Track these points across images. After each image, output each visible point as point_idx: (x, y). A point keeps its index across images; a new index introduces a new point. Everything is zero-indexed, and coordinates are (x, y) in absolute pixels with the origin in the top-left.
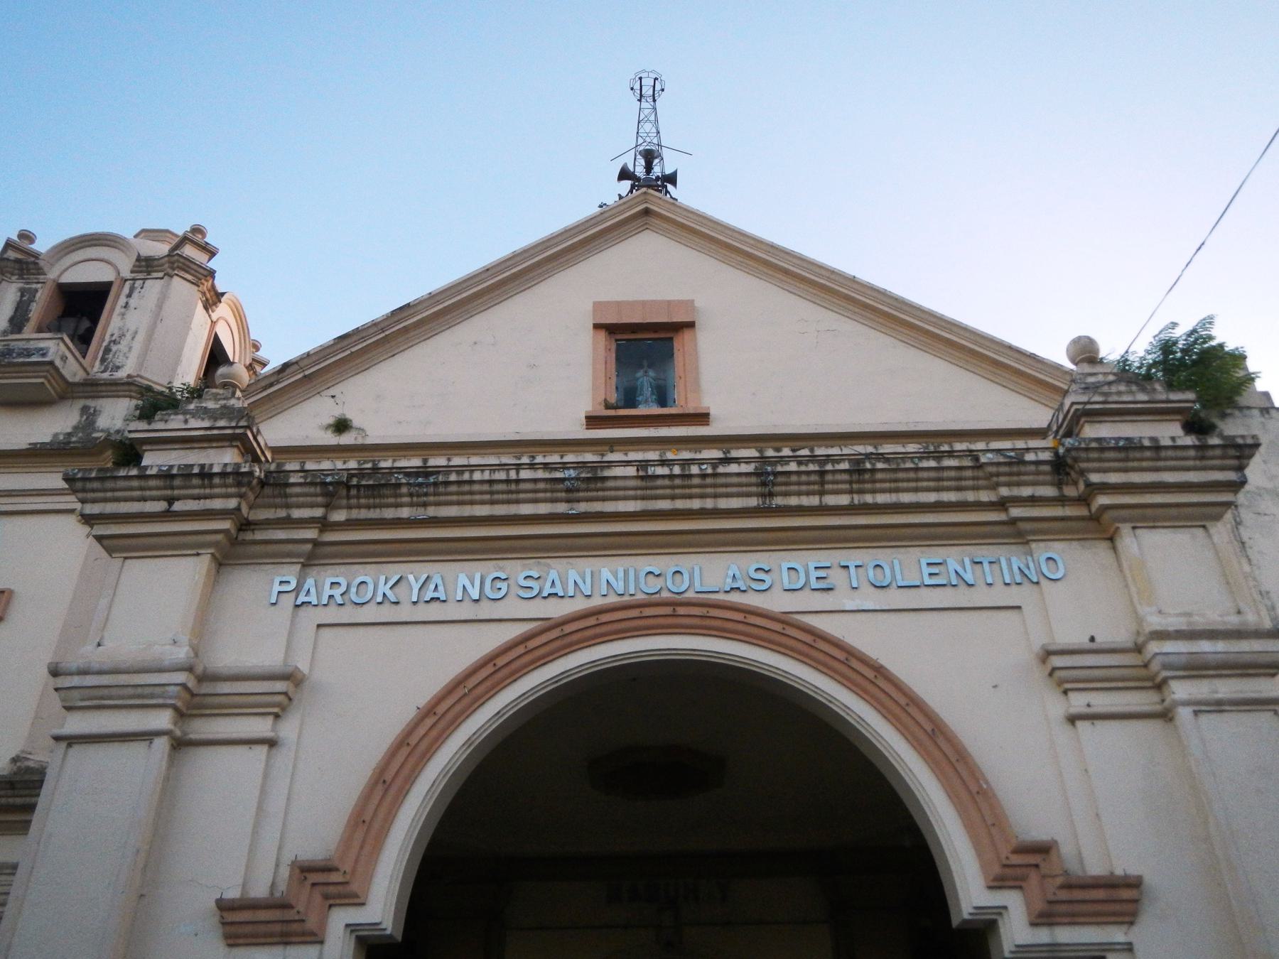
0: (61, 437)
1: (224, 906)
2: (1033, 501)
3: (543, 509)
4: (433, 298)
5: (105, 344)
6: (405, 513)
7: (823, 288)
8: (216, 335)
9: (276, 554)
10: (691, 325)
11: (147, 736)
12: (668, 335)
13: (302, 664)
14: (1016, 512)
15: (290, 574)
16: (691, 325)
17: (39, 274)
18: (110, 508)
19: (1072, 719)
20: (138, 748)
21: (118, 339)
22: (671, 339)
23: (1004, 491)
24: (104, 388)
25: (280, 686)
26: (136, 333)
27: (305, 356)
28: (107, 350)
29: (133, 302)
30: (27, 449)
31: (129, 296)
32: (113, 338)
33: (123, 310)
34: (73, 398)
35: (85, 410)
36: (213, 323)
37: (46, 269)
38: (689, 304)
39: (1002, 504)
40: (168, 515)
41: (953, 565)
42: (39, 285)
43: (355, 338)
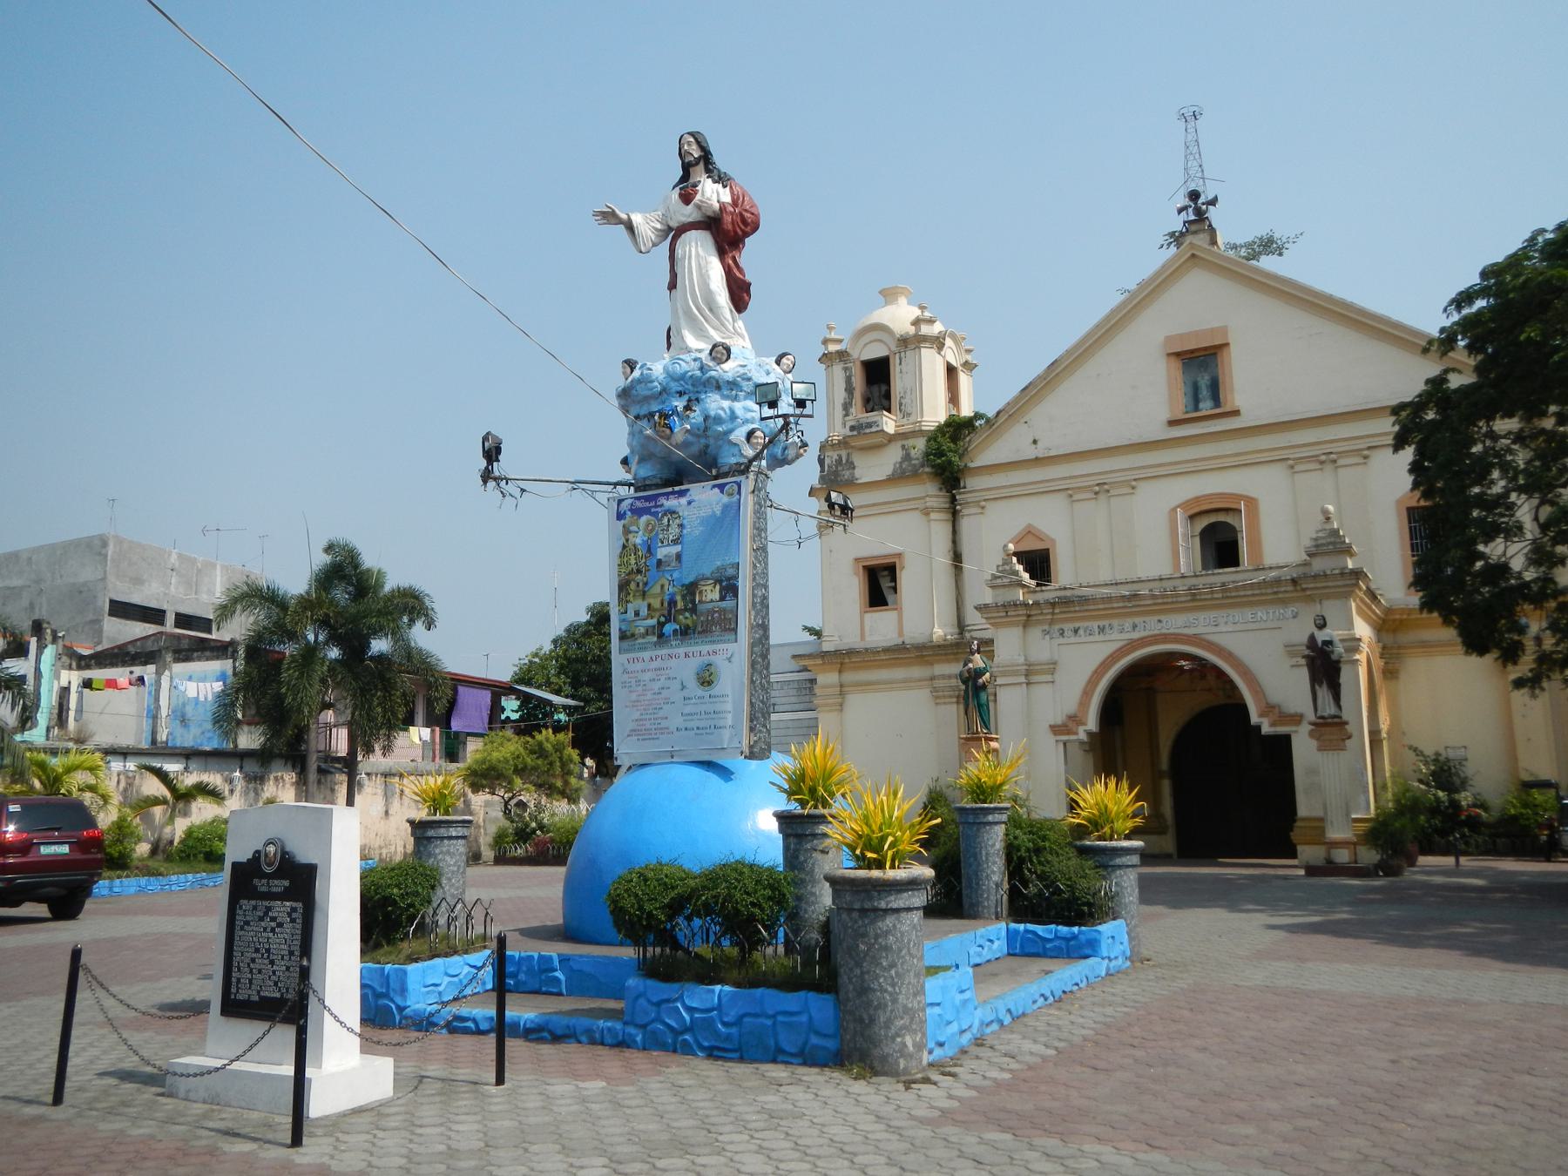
1: (1050, 726)
2: (1286, 592)
3: (1121, 604)
4: (1069, 352)
6: (1077, 609)
7: (1313, 304)
8: (948, 363)
9: (1039, 622)
10: (1227, 345)
11: (1020, 684)
12: (1212, 352)
13: (1056, 658)
14: (1280, 596)
15: (1046, 627)
16: (1227, 345)
18: (990, 615)
19: (1293, 666)
20: (1018, 688)
22: (1215, 354)
23: (1275, 590)
25: (1052, 666)
28: (901, 404)
31: (900, 364)
35: (903, 447)
36: (944, 357)
38: (1224, 330)
39: (1276, 593)
40: (1007, 616)
41: (1259, 614)
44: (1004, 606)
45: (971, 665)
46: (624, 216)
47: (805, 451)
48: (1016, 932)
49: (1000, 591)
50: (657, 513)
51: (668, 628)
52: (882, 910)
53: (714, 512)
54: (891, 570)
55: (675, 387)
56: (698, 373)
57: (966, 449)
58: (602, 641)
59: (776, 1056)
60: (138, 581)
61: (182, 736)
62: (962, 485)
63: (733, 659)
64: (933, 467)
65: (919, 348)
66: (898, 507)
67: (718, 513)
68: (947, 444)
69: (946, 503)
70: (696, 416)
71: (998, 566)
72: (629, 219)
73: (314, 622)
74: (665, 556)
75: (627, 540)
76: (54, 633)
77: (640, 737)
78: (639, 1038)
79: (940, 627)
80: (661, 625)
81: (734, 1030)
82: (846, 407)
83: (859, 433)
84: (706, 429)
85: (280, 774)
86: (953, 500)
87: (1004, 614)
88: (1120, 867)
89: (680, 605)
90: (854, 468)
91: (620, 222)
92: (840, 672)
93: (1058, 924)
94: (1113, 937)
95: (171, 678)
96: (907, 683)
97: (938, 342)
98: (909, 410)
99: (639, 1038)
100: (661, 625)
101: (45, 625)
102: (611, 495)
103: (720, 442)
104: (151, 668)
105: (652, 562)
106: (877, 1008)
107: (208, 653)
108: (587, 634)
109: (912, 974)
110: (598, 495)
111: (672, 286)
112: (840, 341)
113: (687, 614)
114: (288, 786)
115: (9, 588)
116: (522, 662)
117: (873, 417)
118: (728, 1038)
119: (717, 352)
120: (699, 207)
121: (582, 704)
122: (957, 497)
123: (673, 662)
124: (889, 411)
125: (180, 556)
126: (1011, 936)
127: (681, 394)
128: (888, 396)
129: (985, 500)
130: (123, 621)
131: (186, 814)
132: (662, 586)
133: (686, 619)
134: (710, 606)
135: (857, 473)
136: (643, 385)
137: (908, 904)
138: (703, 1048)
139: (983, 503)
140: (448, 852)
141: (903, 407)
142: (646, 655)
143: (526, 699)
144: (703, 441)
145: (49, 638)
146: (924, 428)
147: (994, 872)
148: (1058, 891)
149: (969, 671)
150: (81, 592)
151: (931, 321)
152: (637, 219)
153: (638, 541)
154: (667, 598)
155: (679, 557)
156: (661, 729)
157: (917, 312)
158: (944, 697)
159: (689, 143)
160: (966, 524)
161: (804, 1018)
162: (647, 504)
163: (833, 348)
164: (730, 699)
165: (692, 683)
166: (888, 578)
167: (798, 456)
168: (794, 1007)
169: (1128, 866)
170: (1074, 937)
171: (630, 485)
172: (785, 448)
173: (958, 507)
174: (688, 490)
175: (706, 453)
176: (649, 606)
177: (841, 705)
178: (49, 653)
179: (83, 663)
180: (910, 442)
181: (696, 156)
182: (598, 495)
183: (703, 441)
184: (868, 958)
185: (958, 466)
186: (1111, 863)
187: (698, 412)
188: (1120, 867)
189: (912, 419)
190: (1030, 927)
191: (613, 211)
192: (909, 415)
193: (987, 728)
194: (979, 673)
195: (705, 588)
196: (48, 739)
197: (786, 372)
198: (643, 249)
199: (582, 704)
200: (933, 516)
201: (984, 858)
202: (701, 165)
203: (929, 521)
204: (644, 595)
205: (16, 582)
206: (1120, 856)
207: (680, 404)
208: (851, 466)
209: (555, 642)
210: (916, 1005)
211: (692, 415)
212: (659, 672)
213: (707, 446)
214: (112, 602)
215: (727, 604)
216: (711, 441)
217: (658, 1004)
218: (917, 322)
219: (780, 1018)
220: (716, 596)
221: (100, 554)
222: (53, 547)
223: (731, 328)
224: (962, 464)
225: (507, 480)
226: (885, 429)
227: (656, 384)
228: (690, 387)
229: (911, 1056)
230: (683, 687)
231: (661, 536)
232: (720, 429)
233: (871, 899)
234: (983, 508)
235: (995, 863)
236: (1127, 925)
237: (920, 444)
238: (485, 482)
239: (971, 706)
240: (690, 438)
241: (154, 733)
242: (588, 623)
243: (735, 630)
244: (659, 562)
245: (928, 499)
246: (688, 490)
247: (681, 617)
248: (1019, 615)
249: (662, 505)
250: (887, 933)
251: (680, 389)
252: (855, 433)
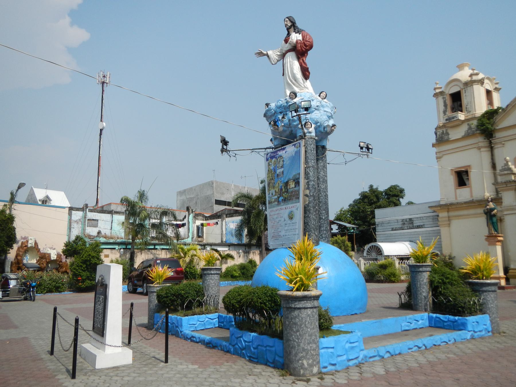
0: (466, 132)
5: (465, 106)
26: (470, 102)
28: (466, 108)
29: (467, 94)
31: (465, 93)
33: (465, 97)
35: (468, 124)
40: (507, 186)
44: (505, 182)
45: (488, 207)
46: (265, 53)
47: (335, 128)
48: (432, 317)
49: (504, 177)
50: (277, 157)
51: (281, 199)
52: (293, 308)
53: (292, 155)
54: (467, 172)
55: (278, 110)
56: (286, 104)
57: (494, 122)
58: (364, 205)
59: (266, 363)
60: (223, 194)
61: (232, 240)
62: (494, 136)
63: (298, 209)
64: (481, 130)
65: (472, 85)
66: (468, 147)
67: (294, 155)
68: (485, 121)
69: (487, 144)
70: (286, 120)
71: (502, 167)
72: (267, 53)
73: (261, 203)
74: (279, 173)
75: (269, 168)
76: (192, 210)
77: (274, 239)
78: (232, 350)
79: (488, 193)
80: (279, 198)
81: (256, 351)
82: (445, 112)
83: (449, 121)
84: (290, 124)
85: (254, 251)
86: (490, 143)
87: (505, 186)
88: (486, 291)
89: (284, 190)
90: (449, 135)
91: (264, 55)
92: (448, 212)
93: (450, 315)
94: (477, 322)
95: (226, 222)
96: (475, 215)
97: (481, 82)
98: (470, 110)
99: (232, 350)
100: (279, 198)
101: (190, 208)
102: (264, 153)
103: (296, 129)
104: (220, 220)
105: (276, 175)
106: (292, 348)
107: (237, 214)
108: (359, 203)
109: (307, 335)
110: (260, 153)
111: (283, 75)
112: (441, 88)
113: (286, 193)
114: (257, 255)
115: (191, 198)
116: (338, 213)
117: (454, 114)
118: (254, 353)
119: (291, 95)
120: (290, 43)
121: (358, 227)
122: (492, 141)
123: (282, 211)
124: (462, 111)
125: (235, 185)
126: (430, 319)
127: (281, 113)
128: (461, 106)
129: (504, 141)
130: (219, 206)
131: (226, 263)
132: (279, 184)
133: (285, 195)
134: (292, 190)
135: (450, 136)
136: (269, 112)
137: (304, 306)
138: (248, 357)
139: (503, 143)
140: (211, 279)
141: (467, 109)
142: (275, 209)
143: (340, 226)
144: (290, 129)
145: (191, 211)
146: (476, 116)
147: (423, 292)
148: (449, 301)
149: (487, 209)
150: (208, 198)
151: (477, 74)
152: (270, 53)
153: (272, 168)
154: (280, 188)
155: (283, 172)
156: (279, 236)
157: (471, 72)
159: (287, 21)
160: (496, 152)
161: (273, 349)
162: (274, 154)
163: (438, 91)
164: (297, 224)
165: (287, 219)
166: (466, 175)
167: (332, 131)
168: (271, 344)
169: (490, 291)
170: (456, 321)
171: (273, 148)
172: (324, 128)
173: (493, 145)
174: (286, 148)
175: (292, 134)
176: (275, 191)
177: (449, 224)
178: (191, 216)
179: (206, 219)
180: (471, 122)
181: (289, 25)
182: (260, 153)
183: (290, 129)
184: (289, 327)
185: (491, 129)
186: (481, 290)
187: (286, 119)
188: (486, 291)
189: (471, 113)
190: (438, 315)
191: (261, 51)
192: (470, 112)
193: (496, 231)
194: (492, 210)
195: (290, 183)
196: (192, 241)
197: (322, 99)
198: (273, 63)
199: (358, 227)
200: (482, 150)
201: (419, 286)
202: (292, 28)
203: (481, 152)
204: (274, 187)
205: (192, 196)
206: (485, 286)
207: (280, 117)
208: (448, 134)
209: (350, 206)
210: (309, 348)
211: (284, 120)
212: (279, 215)
213: (292, 131)
214: (216, 200)
215: (297, 188)
216: (293, 129)
217: (237, 338)
218: (471, 76)
219: (268, 348)
220: (293, 186)
221: (212, 186)
222: (200, 185)
223: (303, 86)
224: (493, 128)
225: (229, 151)
226: (460, 118)
227: (273, 110)
228: (284, 110)
229: (306, 369)
230: (285, 220)
231: (278, 165)
232: (295, 124)
233: (289, 303)
234: (504, 144)
235: (424, 288)
236: (490, 317)
237: (475, 123)
238: (222, 153)
239: (489, 223)
240: (285, 129)
241: (222, 239)
242: (360, 199)
243: (299, 198)
244: (278, 175)
245: (479, 143)
246: (286, 148)
247: (284, 194)
248: (512, 186)
249: (278, 154)
250: (296, 317)
251: (280, 111)
252: (448, 121)
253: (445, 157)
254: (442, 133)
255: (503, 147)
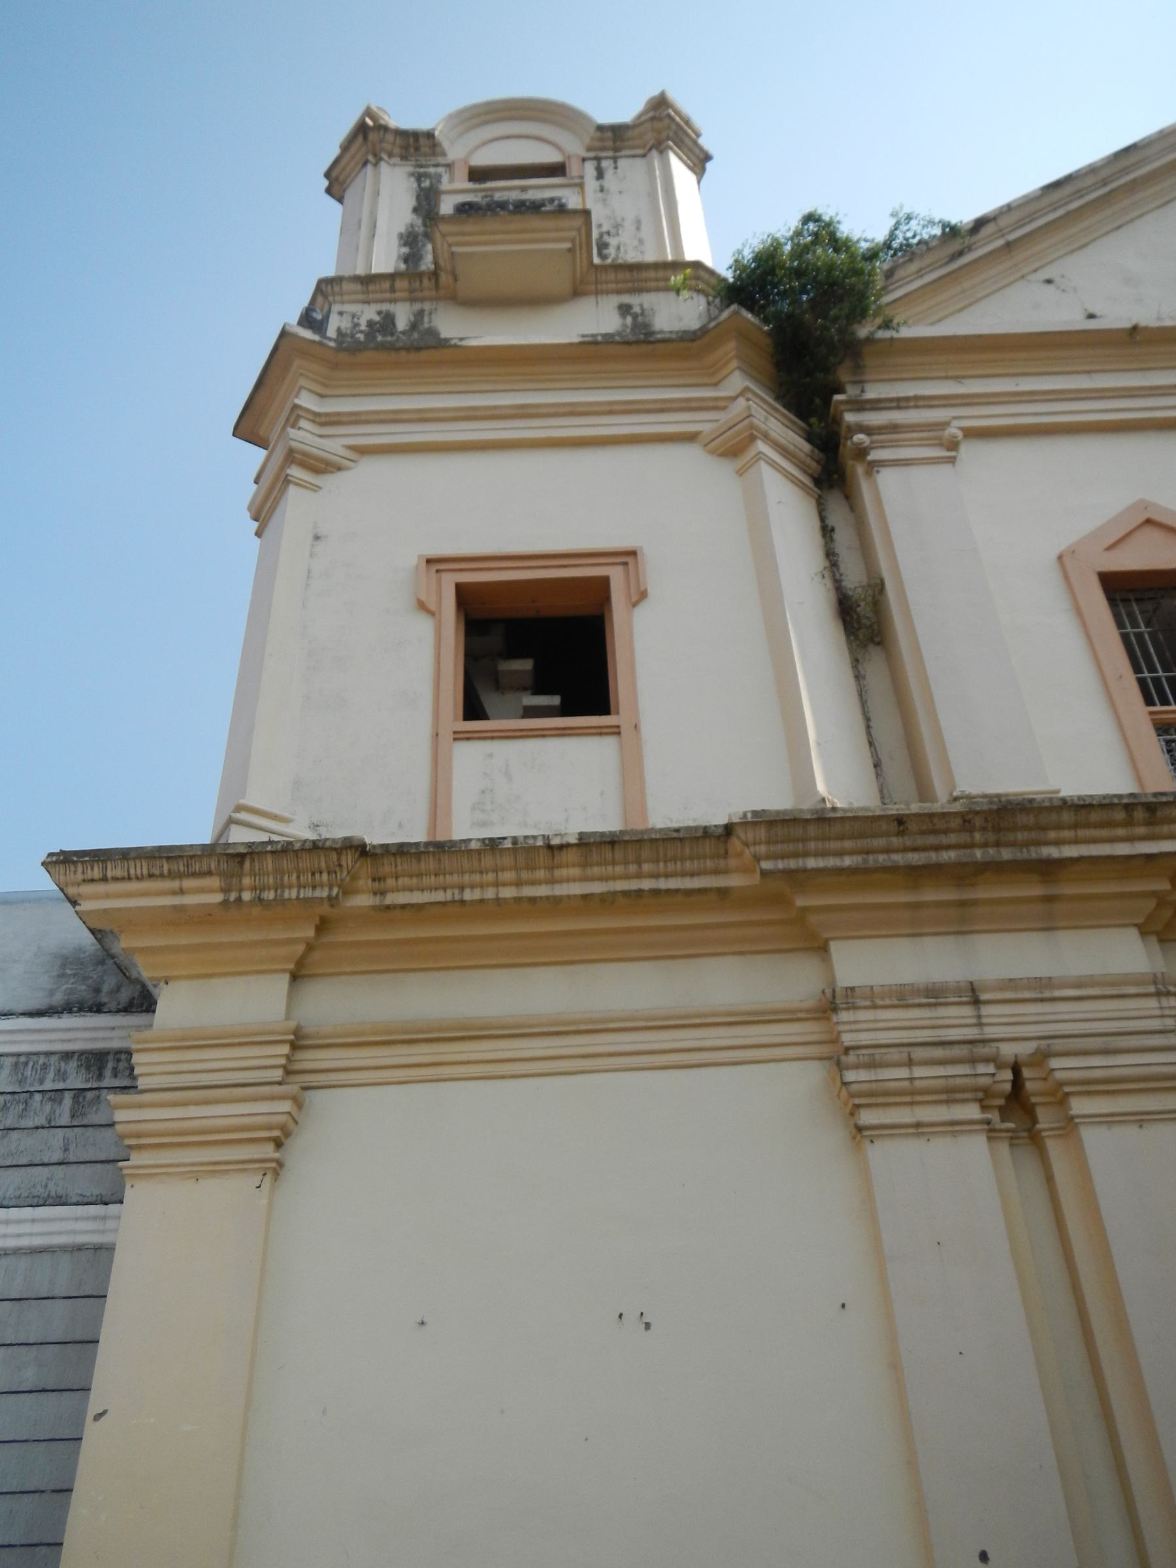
17: (434, 154)
21: (613, 231)
24: (652, 274)
27: (1005, 209)
30: (581, 343)
32: (604, 229)
34: (597, 293)
37: (446, 145)
42: (441, 170)
43: (1068, 190)
158: (912, 1095)
253: (370, 470)
254: (370, 324)
255: (952, 461)
